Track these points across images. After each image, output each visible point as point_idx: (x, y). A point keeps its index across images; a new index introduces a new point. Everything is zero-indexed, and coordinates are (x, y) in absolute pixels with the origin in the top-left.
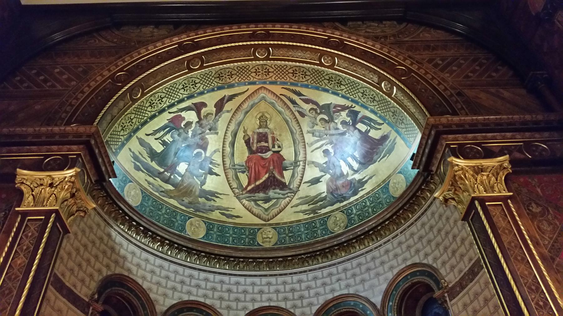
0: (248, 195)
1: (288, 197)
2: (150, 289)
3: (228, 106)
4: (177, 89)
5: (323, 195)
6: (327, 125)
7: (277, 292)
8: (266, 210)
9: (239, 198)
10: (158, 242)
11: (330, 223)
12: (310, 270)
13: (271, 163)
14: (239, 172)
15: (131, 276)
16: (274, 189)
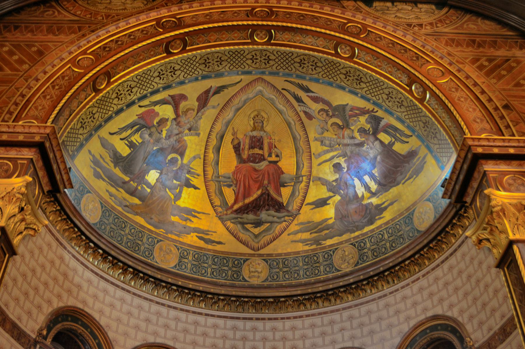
0: (233, 216)
1: (285, 221)
3: (215, 100)
4: (152, 76)
5: (331, 222)
6: (340, 132)
8: (256, 236)
9: (223, 219)
10: (120, 269)
11: (336, 259)
12: (307, 316)
13: (266, 176)
14: (224, 186)
15: (86, 309)
16: (267, 210)
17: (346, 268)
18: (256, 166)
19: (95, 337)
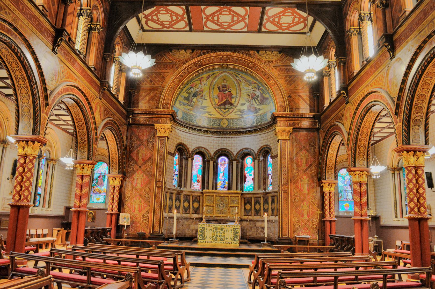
8: (225, 113)
17: (249, 125)
18: (225, 92)
19: (185, 148)
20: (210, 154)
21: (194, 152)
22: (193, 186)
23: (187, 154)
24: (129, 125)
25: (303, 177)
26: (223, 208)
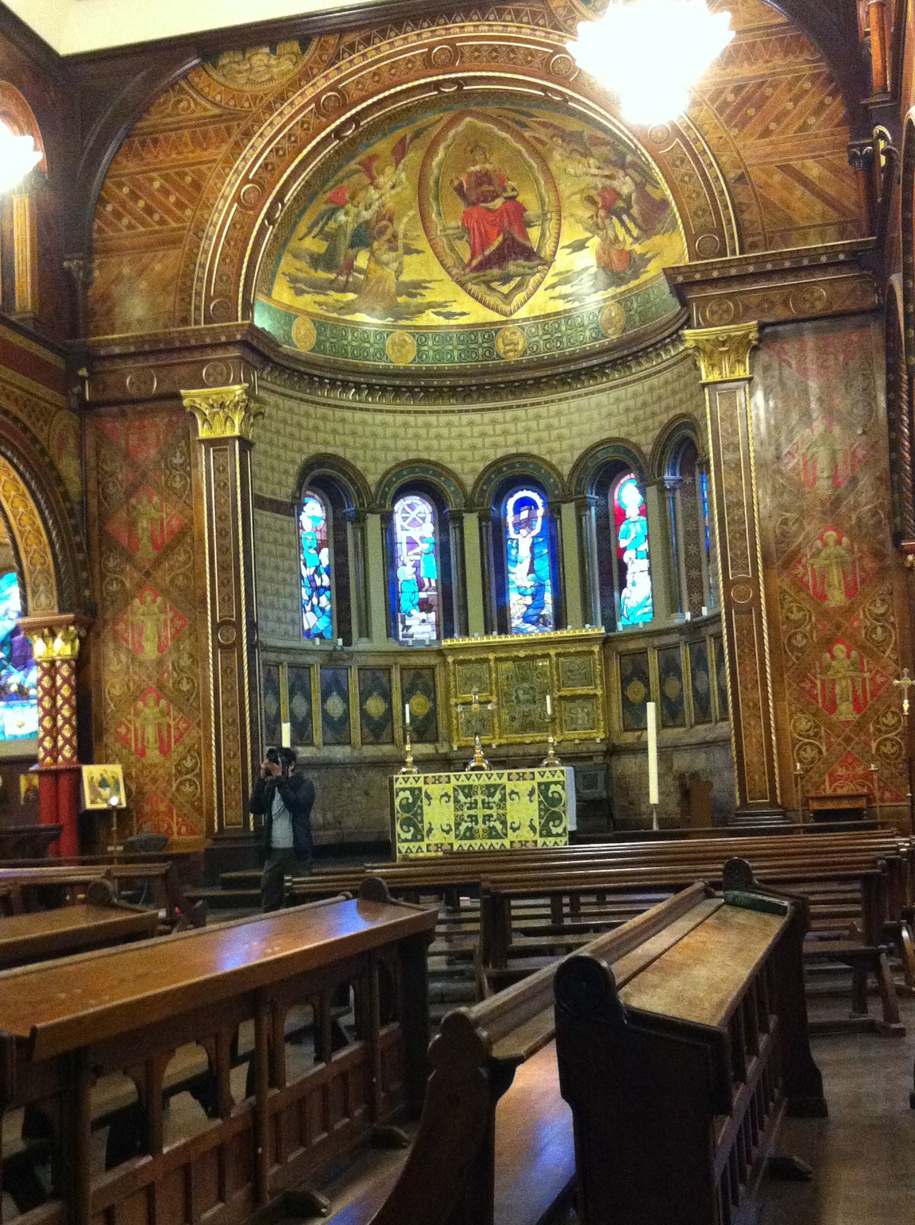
2: (356, 457)
7: (528, 430)
16: (515, 259)
18: (490, 205)
20: (461, 484)
21: (389, 484)
22: (408, 627)
23: (360, 496)
24: (85, 409)
25: (821, 538)
26: (533, 707)
